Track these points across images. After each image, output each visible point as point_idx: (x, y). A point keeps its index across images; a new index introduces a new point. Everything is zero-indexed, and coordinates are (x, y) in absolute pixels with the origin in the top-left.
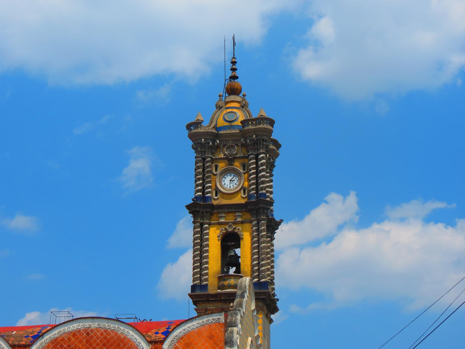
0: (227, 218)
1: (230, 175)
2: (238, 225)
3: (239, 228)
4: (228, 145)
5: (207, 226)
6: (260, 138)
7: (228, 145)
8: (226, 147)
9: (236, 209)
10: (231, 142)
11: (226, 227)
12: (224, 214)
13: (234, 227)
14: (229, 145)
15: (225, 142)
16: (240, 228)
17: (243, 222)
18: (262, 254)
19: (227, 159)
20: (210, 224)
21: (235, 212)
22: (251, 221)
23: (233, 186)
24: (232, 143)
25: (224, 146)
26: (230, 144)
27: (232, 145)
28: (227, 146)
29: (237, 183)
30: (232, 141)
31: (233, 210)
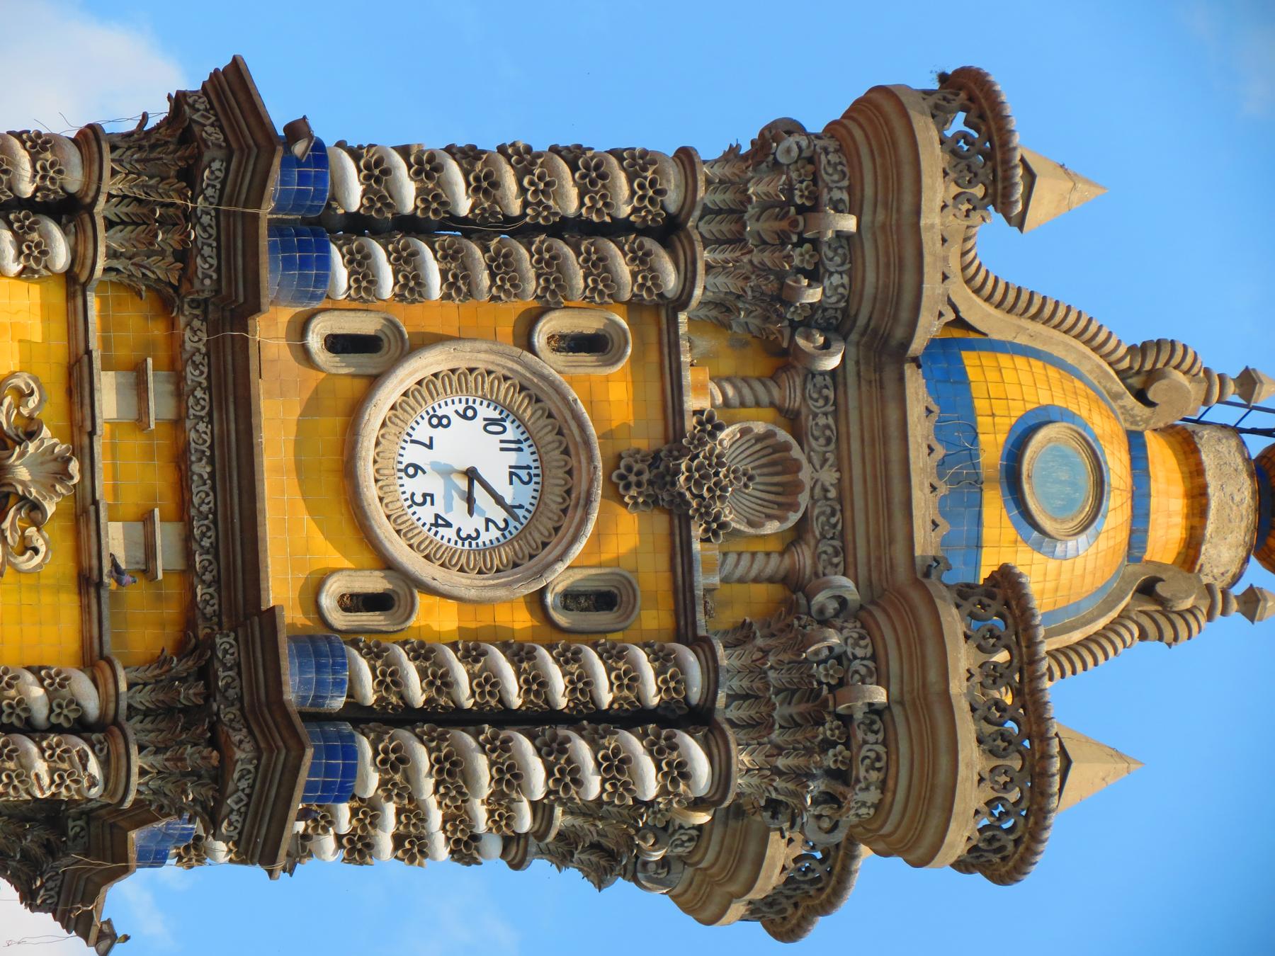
0: (133, 443)
1: (523, 474)
2: (65, 545)
3: (36, 551)
4: (796, 452)
5: (61, 256)
6: (863, 753)
7: (796, 452)
8: (783, 435)
9: (215, 522)
10: (829, 476)
11: (46, 432)
12: (168, 411)
13: (50, 508)
14: (796, 467)
15: (822, 421)
16: (38, 559)
17: (92, 590)
18: (61, 759)
19: (667, 441)
20: (74, 282)
21: (183, 512)
22: (103, 663)
23: (419, 499)
24: (817, 490)
25: (792, 419)
26: (805, 475)
27: (797, 487)
28: (786, 447)
29: (449, 533)
30: (833, 494)
31: (201, 496)
